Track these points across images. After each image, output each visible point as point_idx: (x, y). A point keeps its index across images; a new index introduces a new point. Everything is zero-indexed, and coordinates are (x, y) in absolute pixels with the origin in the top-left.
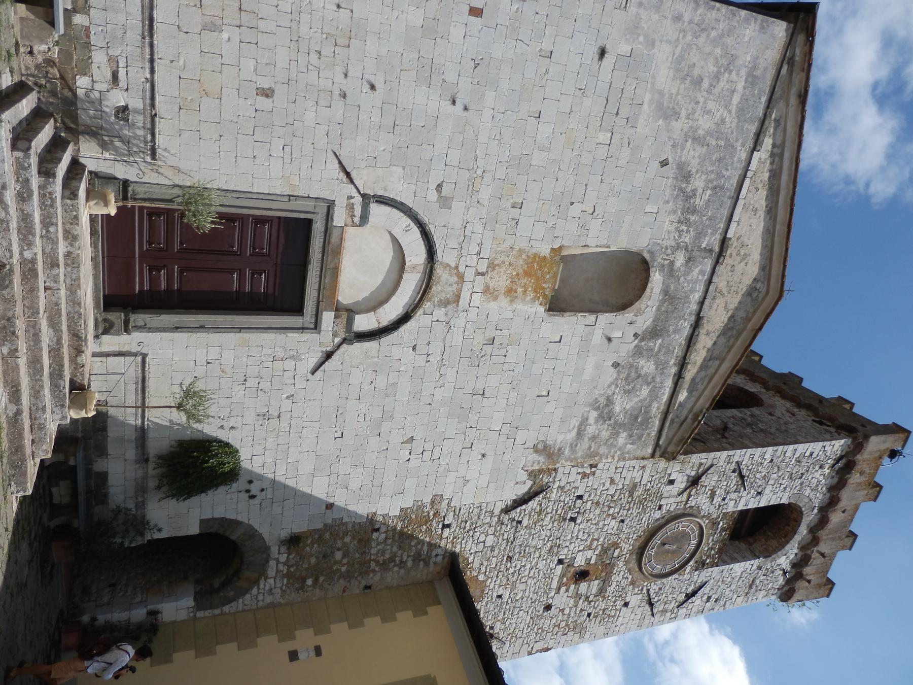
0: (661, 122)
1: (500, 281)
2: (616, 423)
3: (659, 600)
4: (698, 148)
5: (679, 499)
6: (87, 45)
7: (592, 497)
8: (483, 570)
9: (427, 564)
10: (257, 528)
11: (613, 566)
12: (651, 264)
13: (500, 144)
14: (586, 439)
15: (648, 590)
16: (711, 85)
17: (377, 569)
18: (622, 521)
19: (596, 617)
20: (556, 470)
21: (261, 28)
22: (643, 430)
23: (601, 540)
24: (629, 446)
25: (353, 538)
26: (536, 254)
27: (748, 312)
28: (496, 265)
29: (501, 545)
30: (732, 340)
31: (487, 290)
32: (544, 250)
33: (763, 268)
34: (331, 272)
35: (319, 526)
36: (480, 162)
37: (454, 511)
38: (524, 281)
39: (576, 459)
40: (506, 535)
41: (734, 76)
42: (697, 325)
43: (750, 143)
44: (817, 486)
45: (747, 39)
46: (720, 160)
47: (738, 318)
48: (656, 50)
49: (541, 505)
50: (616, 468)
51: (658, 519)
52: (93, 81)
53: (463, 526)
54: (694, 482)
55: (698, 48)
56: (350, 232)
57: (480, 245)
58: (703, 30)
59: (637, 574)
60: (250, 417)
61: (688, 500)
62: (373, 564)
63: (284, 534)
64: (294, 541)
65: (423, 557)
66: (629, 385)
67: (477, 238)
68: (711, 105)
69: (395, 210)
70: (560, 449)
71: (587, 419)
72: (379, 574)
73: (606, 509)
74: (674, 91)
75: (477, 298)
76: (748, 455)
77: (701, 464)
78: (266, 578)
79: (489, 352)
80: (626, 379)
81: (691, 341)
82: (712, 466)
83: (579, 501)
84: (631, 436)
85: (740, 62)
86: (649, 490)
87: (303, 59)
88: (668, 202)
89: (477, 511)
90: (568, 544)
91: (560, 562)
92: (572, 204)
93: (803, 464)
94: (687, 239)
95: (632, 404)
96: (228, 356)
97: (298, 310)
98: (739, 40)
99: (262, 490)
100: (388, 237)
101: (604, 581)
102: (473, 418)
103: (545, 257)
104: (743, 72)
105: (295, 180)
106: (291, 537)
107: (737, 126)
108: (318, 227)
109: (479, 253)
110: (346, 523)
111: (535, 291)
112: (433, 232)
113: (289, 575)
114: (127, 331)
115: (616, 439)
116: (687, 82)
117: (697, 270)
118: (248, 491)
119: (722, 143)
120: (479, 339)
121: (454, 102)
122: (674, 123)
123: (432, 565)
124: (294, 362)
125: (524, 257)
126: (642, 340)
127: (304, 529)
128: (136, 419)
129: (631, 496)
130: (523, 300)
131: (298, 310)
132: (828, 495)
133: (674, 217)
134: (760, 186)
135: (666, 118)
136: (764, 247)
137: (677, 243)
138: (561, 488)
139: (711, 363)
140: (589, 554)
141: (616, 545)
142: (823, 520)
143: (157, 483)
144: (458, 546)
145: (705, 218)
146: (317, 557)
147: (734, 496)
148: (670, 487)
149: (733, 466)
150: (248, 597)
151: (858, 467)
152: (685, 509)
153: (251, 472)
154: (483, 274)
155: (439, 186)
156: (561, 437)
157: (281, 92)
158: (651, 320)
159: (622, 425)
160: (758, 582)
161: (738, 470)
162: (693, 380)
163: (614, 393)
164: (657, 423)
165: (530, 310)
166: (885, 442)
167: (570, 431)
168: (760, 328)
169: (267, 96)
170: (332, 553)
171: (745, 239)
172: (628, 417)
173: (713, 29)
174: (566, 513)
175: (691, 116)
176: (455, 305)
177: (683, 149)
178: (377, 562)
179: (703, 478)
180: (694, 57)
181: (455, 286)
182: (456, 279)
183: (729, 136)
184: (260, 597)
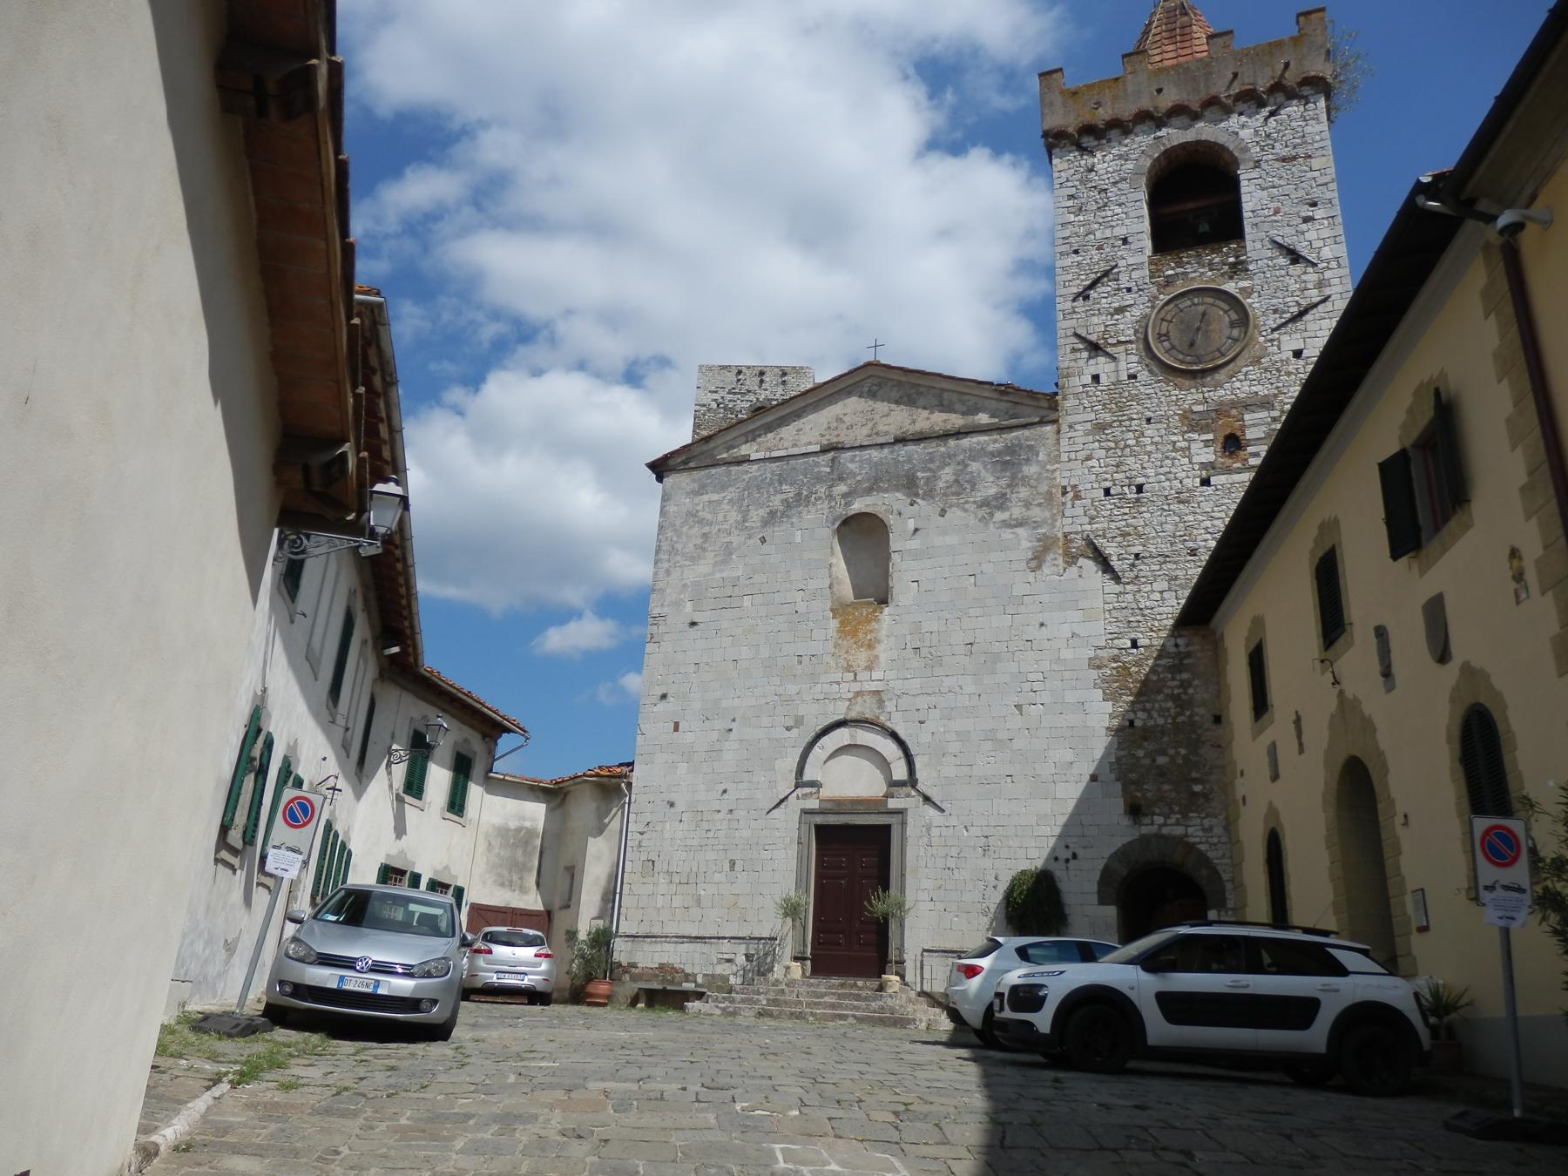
1: (862, 657)
3: (1298, 304)
6: (713, 976)
9: (1188, 655)
11: (1221, 403)
18: (1149, 420)
23: (1174, 438)
24: (1042, 457)
25: (1140, 747)
32: (834, 624)
33: (849, 394)
34: (857, 805)
35: (1119, 786)
41: (700, 507)
42: (901, 440)
43: (745, 467)
44: (1120, 157)
51: (1151, 372)
54: (1095, 348)
56: (825, 793)
57: (831, 683)
59: (1240, 362)
60: (986, 863)
62: (1180, 719)
63: (1126, 821)
64: (1135, 811)
67: (827, 688)
68: (720, 517)
70: (1039, 540)
75: (876, 675)
77: (1074, 350)
78: (1186, 835)
81: (920, 438)
82: (1076, 335)
84: (1028, 460)
87: (710, 842)
89: (1115, 614)
90: (1176, 484)
91: (1206, 482)
94: (822, 490)
96: (926, 884)
97: (888, 828)
102: (996, 647)
103: (842, 623)
104: (696, 500)
105: (788, 840)
108: (819, 820)
110: (1118, 759)
114: (903, 962)
117: (852, 466)
118: (1067, 861)
120: (916, 663)
131: (888, 828)
132: (1138, 129)
136: (831, 403)
142: (1180, 112)
147: (1124, 278)
148: (1103, 379)
149: (1080, 301)
150: (1210, 854)
151: (1087, 117)
153: (1047, 860)
155: (788, 729)
156: (1025, 541)
159: (1013, 478)
160: (1285, 152)
161: (1084, 295)
162: (963, 414)
166: (1051, 104)
178: (1178, 714)
179: (1093, 338)
182: (859, 700)
184: (1215, 840)
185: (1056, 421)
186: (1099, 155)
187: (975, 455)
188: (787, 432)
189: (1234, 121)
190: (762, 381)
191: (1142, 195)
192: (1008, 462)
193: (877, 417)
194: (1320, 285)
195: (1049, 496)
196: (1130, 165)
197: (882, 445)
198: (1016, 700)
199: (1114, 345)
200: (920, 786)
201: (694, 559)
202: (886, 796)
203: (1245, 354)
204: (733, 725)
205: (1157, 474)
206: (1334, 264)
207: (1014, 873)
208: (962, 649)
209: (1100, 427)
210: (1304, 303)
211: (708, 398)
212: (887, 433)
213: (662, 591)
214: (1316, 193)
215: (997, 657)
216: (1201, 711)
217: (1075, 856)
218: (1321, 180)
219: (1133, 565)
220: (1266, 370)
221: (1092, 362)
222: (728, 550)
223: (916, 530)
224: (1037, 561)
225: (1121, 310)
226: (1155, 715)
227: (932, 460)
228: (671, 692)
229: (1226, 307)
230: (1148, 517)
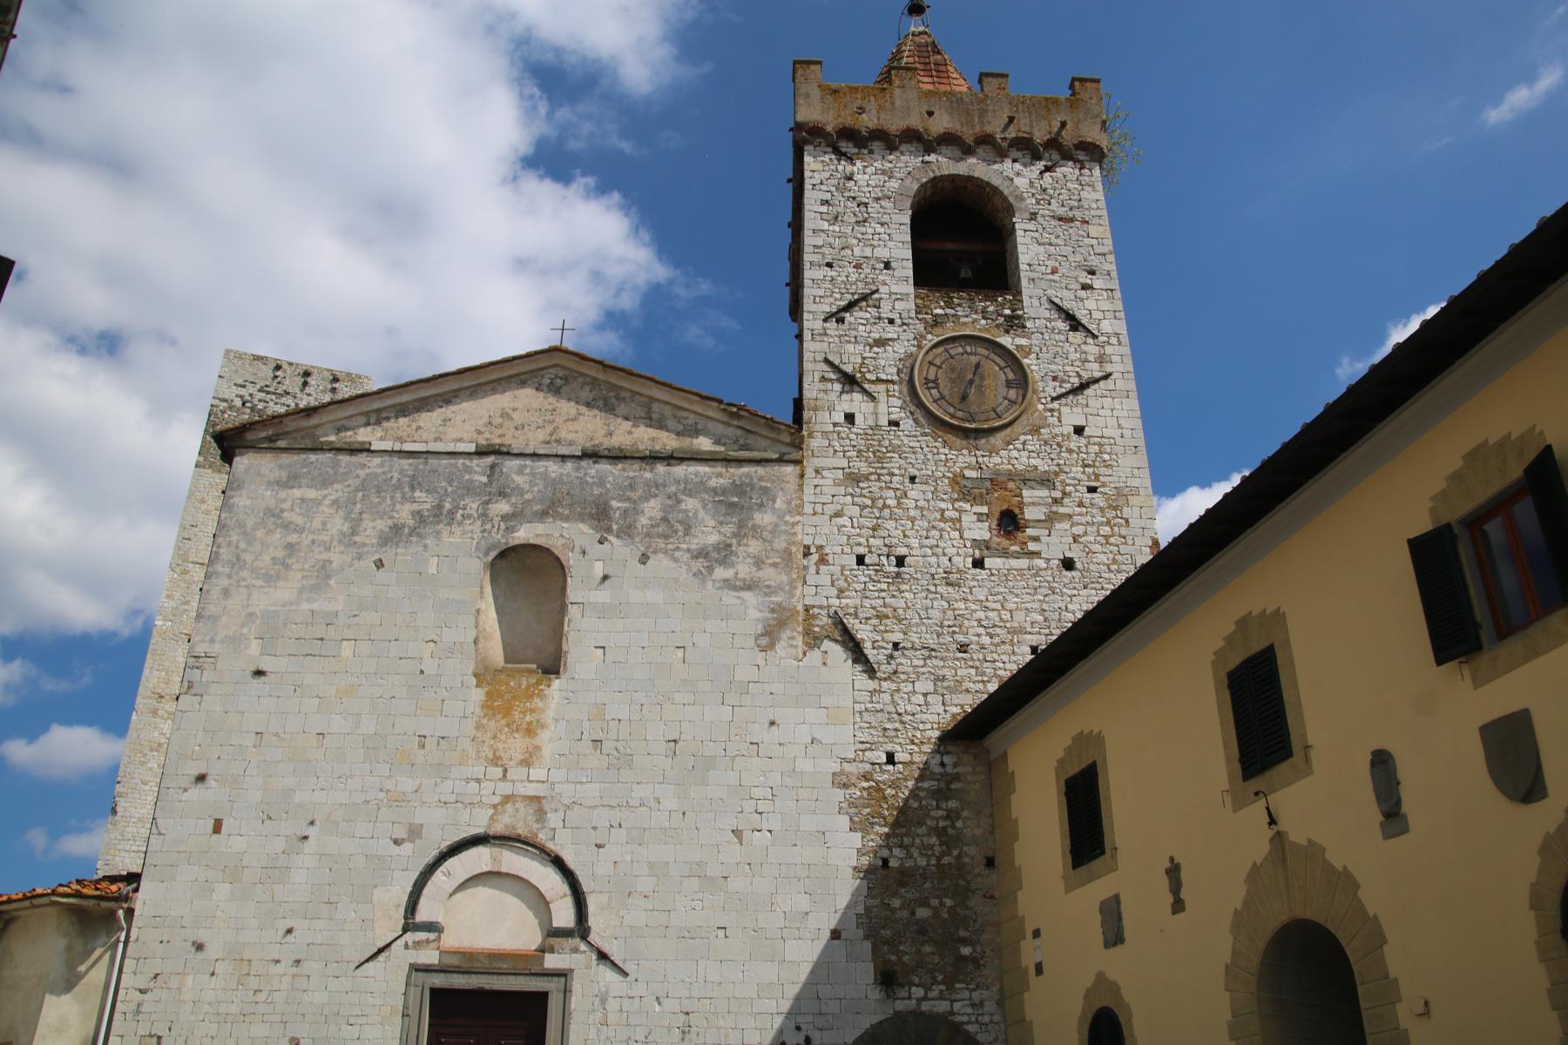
0: (332, 582)
1: (516, 746)
3: (1079, 376)
4: (363, 525)
7: (863, 540)
8: (981, 686)
9: (957, 777)
10: (859, 1033)
11: (997, 473)
12: (504, 547)
13: (351, 776)
14: (760, 574)
15: (1053, 399)
17: (955, 853)
18: (913, 479)
19: (1097, 476)
23: (943, 505)
24: (779, 504)
25: (895, 895)
27: (584, 384)
29: (934, 667)
30: (624, 394)
32: (478, 695)
33: (523, 383)
34: (497, 961)
35: (868, 945)
38: (517, 715)
39: (792, 582)
40: (916, 662)
41: (285, 506)
42: (592, 455)
43: (362, 458)
44: (884, 172)
45: (248, 502)
46: (379, 491)
47: (591, 396)
48: (257, 610)
50: (815, 514)
51: (916, 421)
53: (892, 733)
54: (850, 381)
56: (450, 940)
57: (467, 780)
58: (238, 559)
59: (1017, 427)
61: (887, 381)
62: (946, 860)
63: (876, 994)
64: (888, 980)
65: (943, 785)
66: (676, 532)
68: (317, 524)
69: (425, 892)
70: (773, 611)
71: (726, 580)
72: (966, 848)
73: (886, 512)
74: (299, 575)
75: (536, 773)
77: (823, 379)
78: (952, 1013)
79: (613, 744)
80: (666, 537)
81: (617, 456)
82: (827, 361)
83: (867, 560)
84: (761, 505)
85: (272, 503)
86: (859, 451)
87: (262, 1008)
88: (426, 546)
89: (867, 717)
90: (945, 560)
91: (978, 564)
93: (840, 210)
94: (473, 506)
95: (708, 518)
97: (542, 997)
99: (798, 1028)
100: (459, 896)
101: (1025, 481)
103: (488, 694)
104: (283, 494)
106: (882, 983)
107: (342, 481)
108: (439, 981)
109: (478, 781)
110: (868, 909)
111: (532, 697)
113: (950, 983)
115: (763, 528)
116: (290, 561)
117: (519, 479)
121: (306, 838)
123: (960, 769)
126: (609, 530)
127: (870, 967)
130: (542, 711)
131: (542, 997)
132: (903, 147)
133: (445, 534)
134: (414, 426)
135: (328, 577)
136: (494, 391)
138: (841, 593)
139: (655, 416)
140: (968, 519)
141: (956, 480)
142: (948, 140)
144: (929, 733)
146: (923, 944)
148: (859, 419)
149: (832, 324)
150: (979, 1037)
151: (849, 121)
152: (901, 382)
154: (505, 771)
155: (397, 842)
156: (754, 610)
158: (581, 525)
159: (741, 525)
160: (1061, 211)
161: (837, 317)
162: (678, 434)
164: (745, 470)
166: (807, 96)
167: (744, 601)
168: (600, 363)
170: (918, 922)
171: (481, 422)
177: (364, 545)
178: (943, 854)
179: (848, 369)
181: (518, 805)
182: (509, 807)
184: (986, 1019)
185: (798, 462)
186: (859, 164)
188: (429, 420)
189: (1007, 166)
190: (305, 384)
191: (906, 218)
193: (559, 420)
194: (1101, 359)
195: (787, 553)
196: (894, 184)
197: (563, 458)
198: (731, 822)
199: (872, 382)
200: (593, 937)
202: (542, 950)
203: (1023, 420)
204: (311, 831)
205: (922, 546)
206: (1114, 340)
208: (662, 747)
209: (854, 479)
210: (1085, 375)
211: (232, 393)
212: (571, 443)
213: (214, 619)
214: (1095, 261)
216: (971, 850)
218: (1099, 249)
219: (891, 657)
220: (1046, 443)
221: (845, 397)
222: (324, 572)
223: (605, 578)
224: (769, 637)
225: (881, 343)
226: (916, 854)
227: (632, 487)
228: (212, 774)
229: (1002, 364)
230: (909, 598)
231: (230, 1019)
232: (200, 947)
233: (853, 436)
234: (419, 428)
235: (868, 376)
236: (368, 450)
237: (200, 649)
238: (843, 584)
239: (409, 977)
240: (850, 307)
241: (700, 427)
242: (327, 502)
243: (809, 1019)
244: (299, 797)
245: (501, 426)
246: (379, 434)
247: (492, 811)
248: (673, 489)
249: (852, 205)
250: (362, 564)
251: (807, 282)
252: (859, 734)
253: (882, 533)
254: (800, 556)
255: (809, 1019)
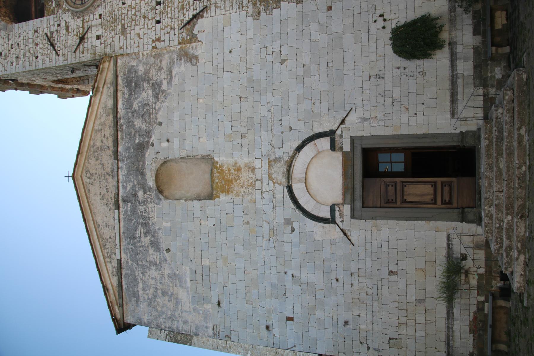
0: (177, 272)
1: (246, 176)
2: (148, 82)
4: (152, 260)
5: (89, 23)
12: (157, 192)
14: (165, 68)
16: (156, 292)
20: (180, 43)
21: (396, 303)
22: (129, 77)
24: (135, 64)
26: (228, 194)
27: (89, 163)
28: (249, 186)
30: (92, 144)
31: (253, 170)
32: (223, 197)
36: (272, 245)
37: (243, 7)
38: (231, 177)
39: (168, 52)
45: (146, 315)
46: (138, 254)
47: (94, 159)
48: (192, 307)
49: (184, 14)
50: (139, 46)
51: (98, 6)
52: (477, 271)
55: (170, 309)
56: (339, 200)
57: (263, 198)
60: (388, 76)
61: (83, 23)
66: (148, 110)
68: (153, 282)
69: (316, 215)
70: (181, 59)
71: (168, 83)
73: (138, 13)
74: (175, 288)
75: (258, 164)
76: (54, 62)
77: (83, 53)
80: (150, 114)
82: (75, 52)
83: (158, 19)
84: (135, 72)
85: (146, 304)
87: (375, 290)
88: (159, 229)
89: (227, 8)
92: (214, 225)
94: (141, 208)
98: (150, 314)
99: (375, 21)
102: (244, 81)
103: (222, 192)
104: (142, 299)
107: (134, 272)
108: (358, 204)
109: (262, 193)
111: (223, 170)
112: (292, 204)
115: (145, 69)
116: (170, 293)
117: (129, 188)
118: (385, 20)
119: (139, 262)
121: (293, 276)
122: (170, 272)
124: (365, 116)
125: (235, 192)
128: (457, 74)
129: (123, 25)
133: (153, 220)
134: (110, 240)
135: (175, 274)
137: (145, 205)
139: (100, 129)
143: (443, 28)
145: (134, 220)
147: (53, 29)
148: (99, 33)
152: (83, 16)
154: (257, 180)
155: (293, 230)
156: (181, 69)
157: (385, 274)
158: (146, 156)
159: (144, 80)
163: (155, 103)
165: (224, 158)
167: (177, 73)
169: (392, 272)
171: (106, 209)
172: (141, 86)
173: (165, 319)
174: (164, 9)
175: (161, 276)
176: (271, 159)
177: (160, 258)
179: (78, 41)
180: (170, 305)
181: (273, 172)
182: (274, 176)
183: (137, 266)
187: (129, 104)
192: (134, 83)
193: (104, 172)
198: (277, 65)
200: (334, 128)
201: (178, 302)
204: (290, 273)
207: (395, 56)
209: (124, 31)
212: (112, 165)
213: (197, 327)
215: (250, 80)
217: (381, 16)
222: (173, 276)
223: (168, 141)
224: (192, 59)
225: (67, 28)
227: (130, 134)
231: (380, 306)
232: (346, 323)
233: (106, 35)
234: (110, 238)
235: (81, 32)
236: (121, 260)
237: (210, 332)
238: (168, 29)
239: (357, 219)
240: (52, 45)
241: (104, 106)
242: (144, 278)
243: (370, 16)
244: (274, 281)
245: (107, 199)
246: (114, 256)
247: (276, 184)
248: (130, 114)
249: (12, 51)
250: (168, 259)
251: (44, 66)
252: (235, 11)
253: (146, 14)
254: (157, 50)
255: (370, 16)
